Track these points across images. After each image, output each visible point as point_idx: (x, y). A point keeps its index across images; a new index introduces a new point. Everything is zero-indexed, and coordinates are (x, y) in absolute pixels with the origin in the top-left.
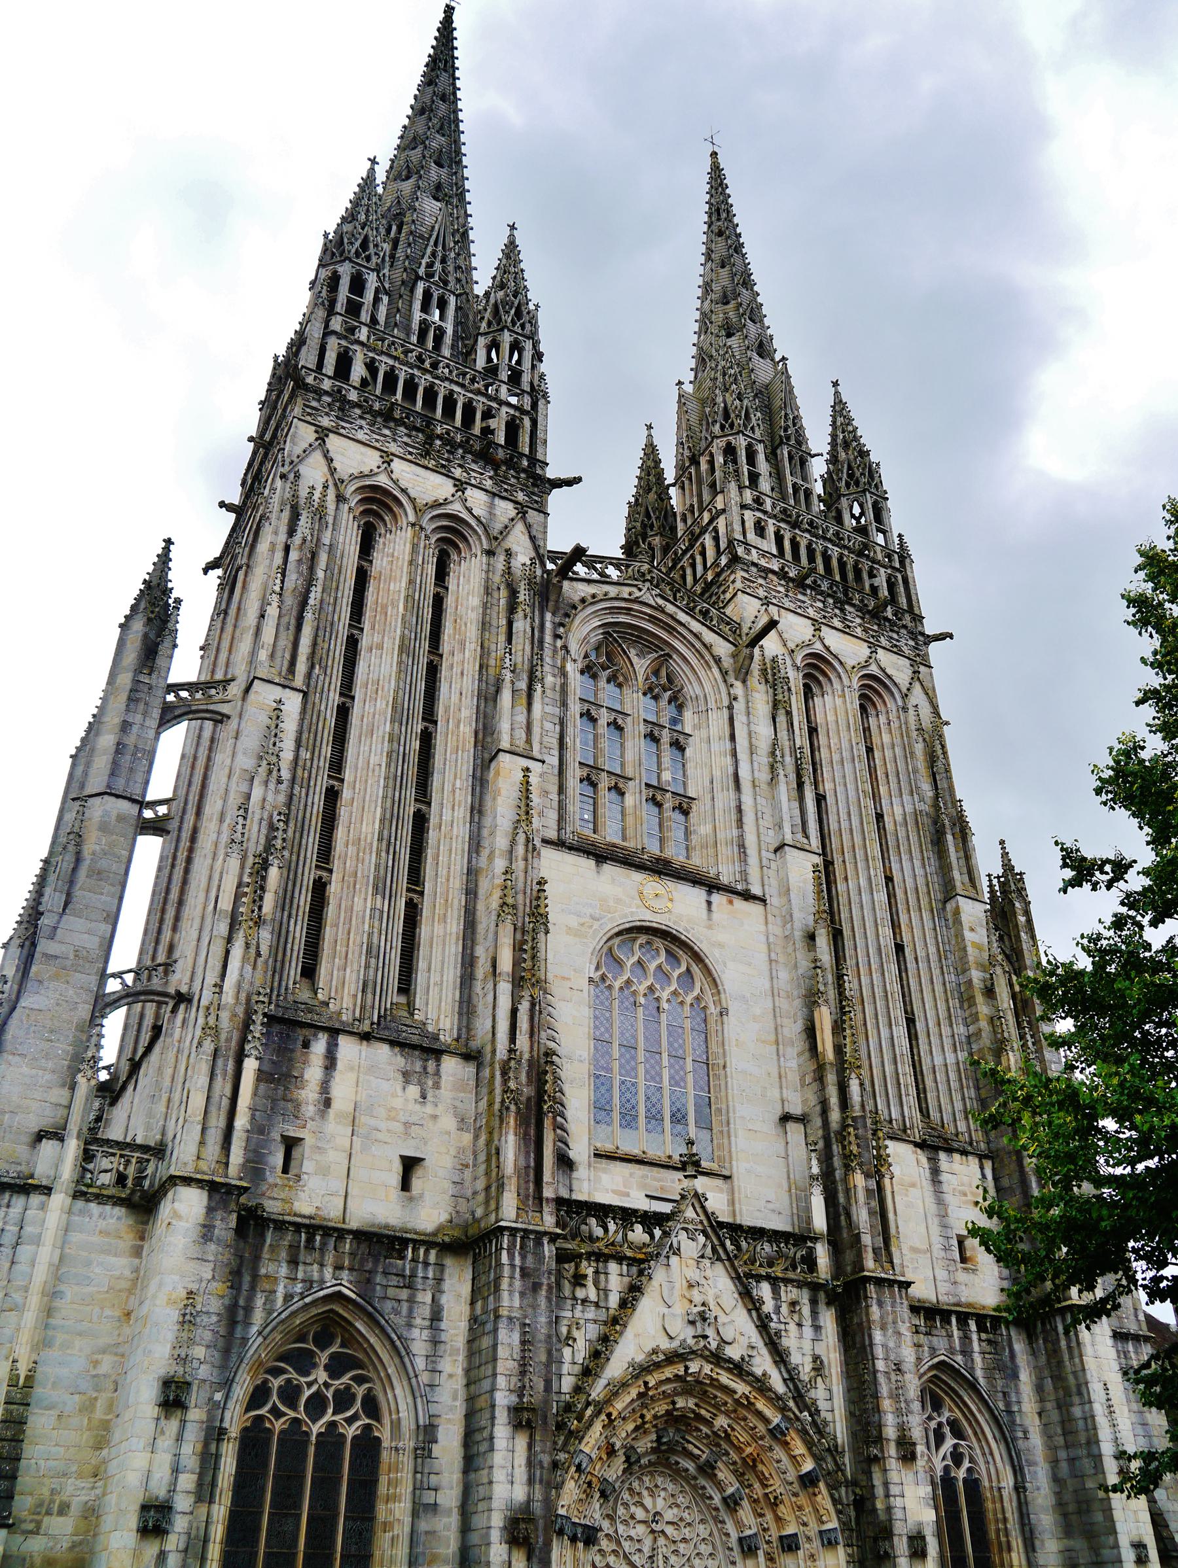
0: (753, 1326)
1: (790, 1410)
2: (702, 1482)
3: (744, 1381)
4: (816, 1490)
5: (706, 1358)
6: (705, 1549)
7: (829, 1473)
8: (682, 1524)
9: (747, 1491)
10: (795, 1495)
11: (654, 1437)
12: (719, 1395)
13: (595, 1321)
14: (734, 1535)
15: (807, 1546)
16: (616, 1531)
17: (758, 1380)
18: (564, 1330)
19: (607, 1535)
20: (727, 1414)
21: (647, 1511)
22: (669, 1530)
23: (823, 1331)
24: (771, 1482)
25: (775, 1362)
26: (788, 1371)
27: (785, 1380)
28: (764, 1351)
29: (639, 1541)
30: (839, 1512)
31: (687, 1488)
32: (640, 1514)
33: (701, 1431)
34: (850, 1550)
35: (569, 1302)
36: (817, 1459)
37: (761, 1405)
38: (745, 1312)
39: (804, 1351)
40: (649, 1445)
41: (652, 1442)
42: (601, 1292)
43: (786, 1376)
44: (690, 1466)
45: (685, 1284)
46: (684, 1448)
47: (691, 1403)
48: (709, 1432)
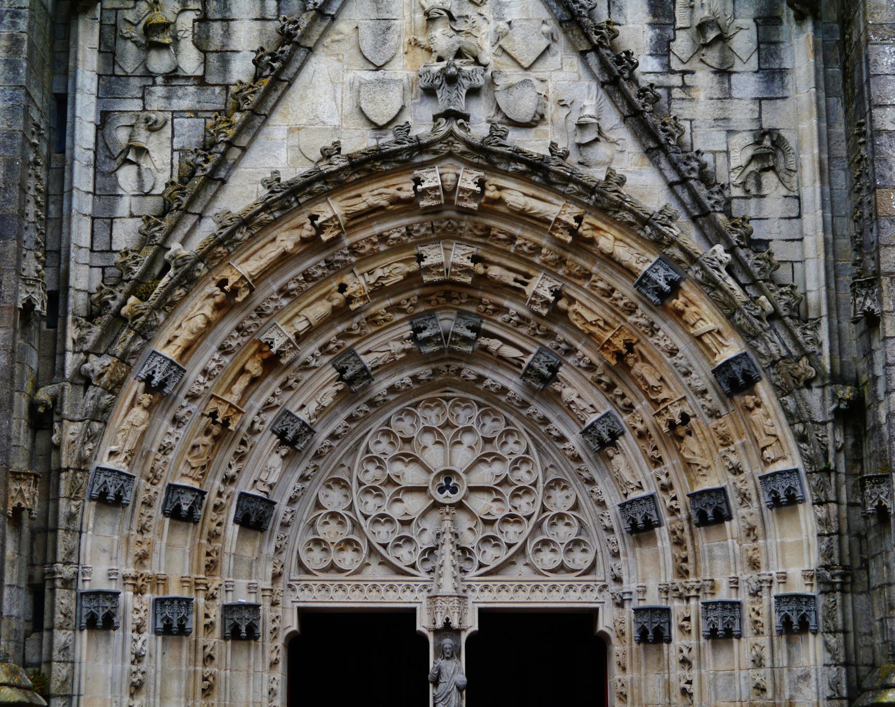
0: (594, 86)
1: (673, 242)
2: (539, 409)
3: (563, 195)
4: (749, 400)
5: (459, 157)
6: (563, 533)
7: (774, 363)
8: (507, 491)
9: (626, 417)
10: (714, 414)
11: (406, 330)
12: (517, 231)
13: (196, 113)
14: (613, 500)
15: (743, 511)
16: (351, 508)
17: (589, 189)
18: (122, 136)
19: (334, 515)
20: (548, 268)
21: (429, 472)
22: (481, 504)
23: (788, 79)
24: (664, 394)
25: (648, 152)
26: (675, 166)
27: (671, 185)
28: (623, 135)
29: (404, 523)
30: (801, 438)
31: (520, 426)
32: (412, 475)
33: (506, 310)
34: (822, 512)
35: (136, 82)
36: (749, 335)
37: (607, 241)
38: (575, 60)
39: (733, 125)
40: (396, 346)
41: (401, 339)
42: (213, 58)
43: (673, 177)
44: (512, 383)
45: (420, 18)
46: (485, 349)
47: (459, 255)
48: (524, 312)
